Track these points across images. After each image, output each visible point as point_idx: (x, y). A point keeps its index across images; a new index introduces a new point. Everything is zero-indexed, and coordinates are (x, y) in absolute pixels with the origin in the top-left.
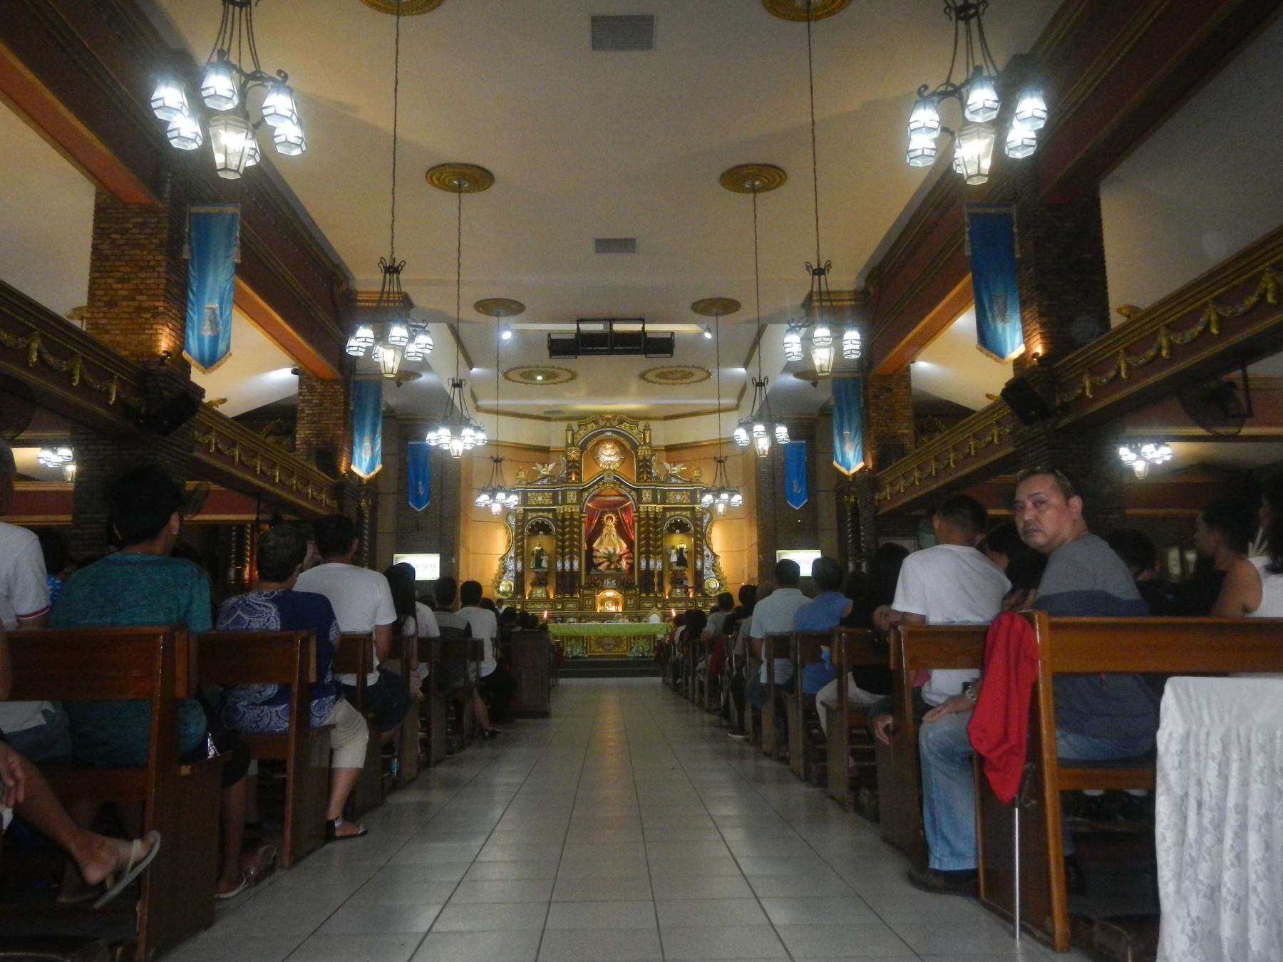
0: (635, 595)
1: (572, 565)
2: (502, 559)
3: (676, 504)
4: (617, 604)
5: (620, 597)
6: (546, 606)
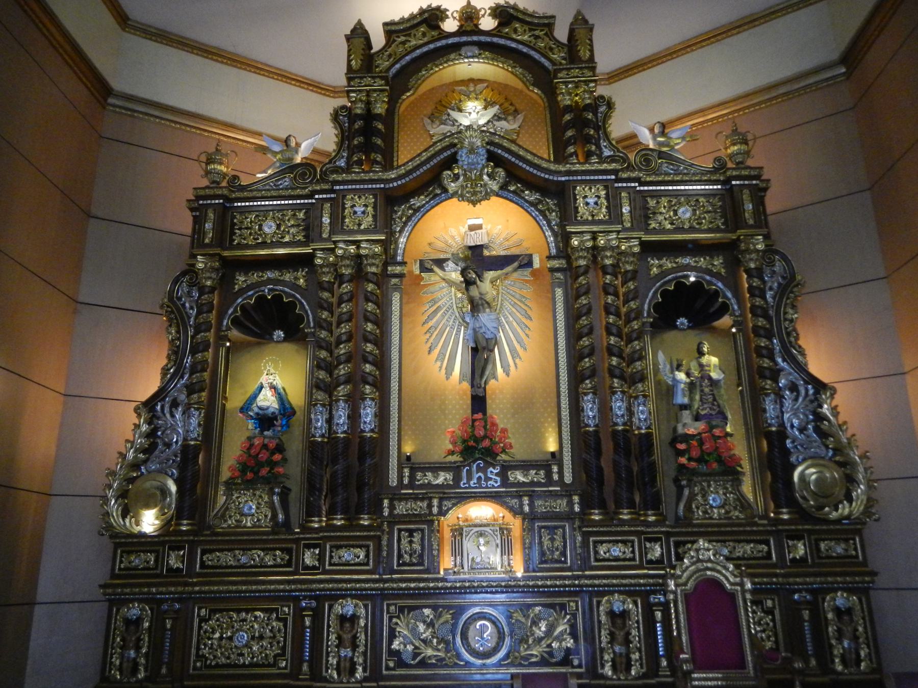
0: (569, 516)
1: (354, 417)
2: (149, 404)
3: (679, 230)
4: (506, 549)
5: (516, 525)
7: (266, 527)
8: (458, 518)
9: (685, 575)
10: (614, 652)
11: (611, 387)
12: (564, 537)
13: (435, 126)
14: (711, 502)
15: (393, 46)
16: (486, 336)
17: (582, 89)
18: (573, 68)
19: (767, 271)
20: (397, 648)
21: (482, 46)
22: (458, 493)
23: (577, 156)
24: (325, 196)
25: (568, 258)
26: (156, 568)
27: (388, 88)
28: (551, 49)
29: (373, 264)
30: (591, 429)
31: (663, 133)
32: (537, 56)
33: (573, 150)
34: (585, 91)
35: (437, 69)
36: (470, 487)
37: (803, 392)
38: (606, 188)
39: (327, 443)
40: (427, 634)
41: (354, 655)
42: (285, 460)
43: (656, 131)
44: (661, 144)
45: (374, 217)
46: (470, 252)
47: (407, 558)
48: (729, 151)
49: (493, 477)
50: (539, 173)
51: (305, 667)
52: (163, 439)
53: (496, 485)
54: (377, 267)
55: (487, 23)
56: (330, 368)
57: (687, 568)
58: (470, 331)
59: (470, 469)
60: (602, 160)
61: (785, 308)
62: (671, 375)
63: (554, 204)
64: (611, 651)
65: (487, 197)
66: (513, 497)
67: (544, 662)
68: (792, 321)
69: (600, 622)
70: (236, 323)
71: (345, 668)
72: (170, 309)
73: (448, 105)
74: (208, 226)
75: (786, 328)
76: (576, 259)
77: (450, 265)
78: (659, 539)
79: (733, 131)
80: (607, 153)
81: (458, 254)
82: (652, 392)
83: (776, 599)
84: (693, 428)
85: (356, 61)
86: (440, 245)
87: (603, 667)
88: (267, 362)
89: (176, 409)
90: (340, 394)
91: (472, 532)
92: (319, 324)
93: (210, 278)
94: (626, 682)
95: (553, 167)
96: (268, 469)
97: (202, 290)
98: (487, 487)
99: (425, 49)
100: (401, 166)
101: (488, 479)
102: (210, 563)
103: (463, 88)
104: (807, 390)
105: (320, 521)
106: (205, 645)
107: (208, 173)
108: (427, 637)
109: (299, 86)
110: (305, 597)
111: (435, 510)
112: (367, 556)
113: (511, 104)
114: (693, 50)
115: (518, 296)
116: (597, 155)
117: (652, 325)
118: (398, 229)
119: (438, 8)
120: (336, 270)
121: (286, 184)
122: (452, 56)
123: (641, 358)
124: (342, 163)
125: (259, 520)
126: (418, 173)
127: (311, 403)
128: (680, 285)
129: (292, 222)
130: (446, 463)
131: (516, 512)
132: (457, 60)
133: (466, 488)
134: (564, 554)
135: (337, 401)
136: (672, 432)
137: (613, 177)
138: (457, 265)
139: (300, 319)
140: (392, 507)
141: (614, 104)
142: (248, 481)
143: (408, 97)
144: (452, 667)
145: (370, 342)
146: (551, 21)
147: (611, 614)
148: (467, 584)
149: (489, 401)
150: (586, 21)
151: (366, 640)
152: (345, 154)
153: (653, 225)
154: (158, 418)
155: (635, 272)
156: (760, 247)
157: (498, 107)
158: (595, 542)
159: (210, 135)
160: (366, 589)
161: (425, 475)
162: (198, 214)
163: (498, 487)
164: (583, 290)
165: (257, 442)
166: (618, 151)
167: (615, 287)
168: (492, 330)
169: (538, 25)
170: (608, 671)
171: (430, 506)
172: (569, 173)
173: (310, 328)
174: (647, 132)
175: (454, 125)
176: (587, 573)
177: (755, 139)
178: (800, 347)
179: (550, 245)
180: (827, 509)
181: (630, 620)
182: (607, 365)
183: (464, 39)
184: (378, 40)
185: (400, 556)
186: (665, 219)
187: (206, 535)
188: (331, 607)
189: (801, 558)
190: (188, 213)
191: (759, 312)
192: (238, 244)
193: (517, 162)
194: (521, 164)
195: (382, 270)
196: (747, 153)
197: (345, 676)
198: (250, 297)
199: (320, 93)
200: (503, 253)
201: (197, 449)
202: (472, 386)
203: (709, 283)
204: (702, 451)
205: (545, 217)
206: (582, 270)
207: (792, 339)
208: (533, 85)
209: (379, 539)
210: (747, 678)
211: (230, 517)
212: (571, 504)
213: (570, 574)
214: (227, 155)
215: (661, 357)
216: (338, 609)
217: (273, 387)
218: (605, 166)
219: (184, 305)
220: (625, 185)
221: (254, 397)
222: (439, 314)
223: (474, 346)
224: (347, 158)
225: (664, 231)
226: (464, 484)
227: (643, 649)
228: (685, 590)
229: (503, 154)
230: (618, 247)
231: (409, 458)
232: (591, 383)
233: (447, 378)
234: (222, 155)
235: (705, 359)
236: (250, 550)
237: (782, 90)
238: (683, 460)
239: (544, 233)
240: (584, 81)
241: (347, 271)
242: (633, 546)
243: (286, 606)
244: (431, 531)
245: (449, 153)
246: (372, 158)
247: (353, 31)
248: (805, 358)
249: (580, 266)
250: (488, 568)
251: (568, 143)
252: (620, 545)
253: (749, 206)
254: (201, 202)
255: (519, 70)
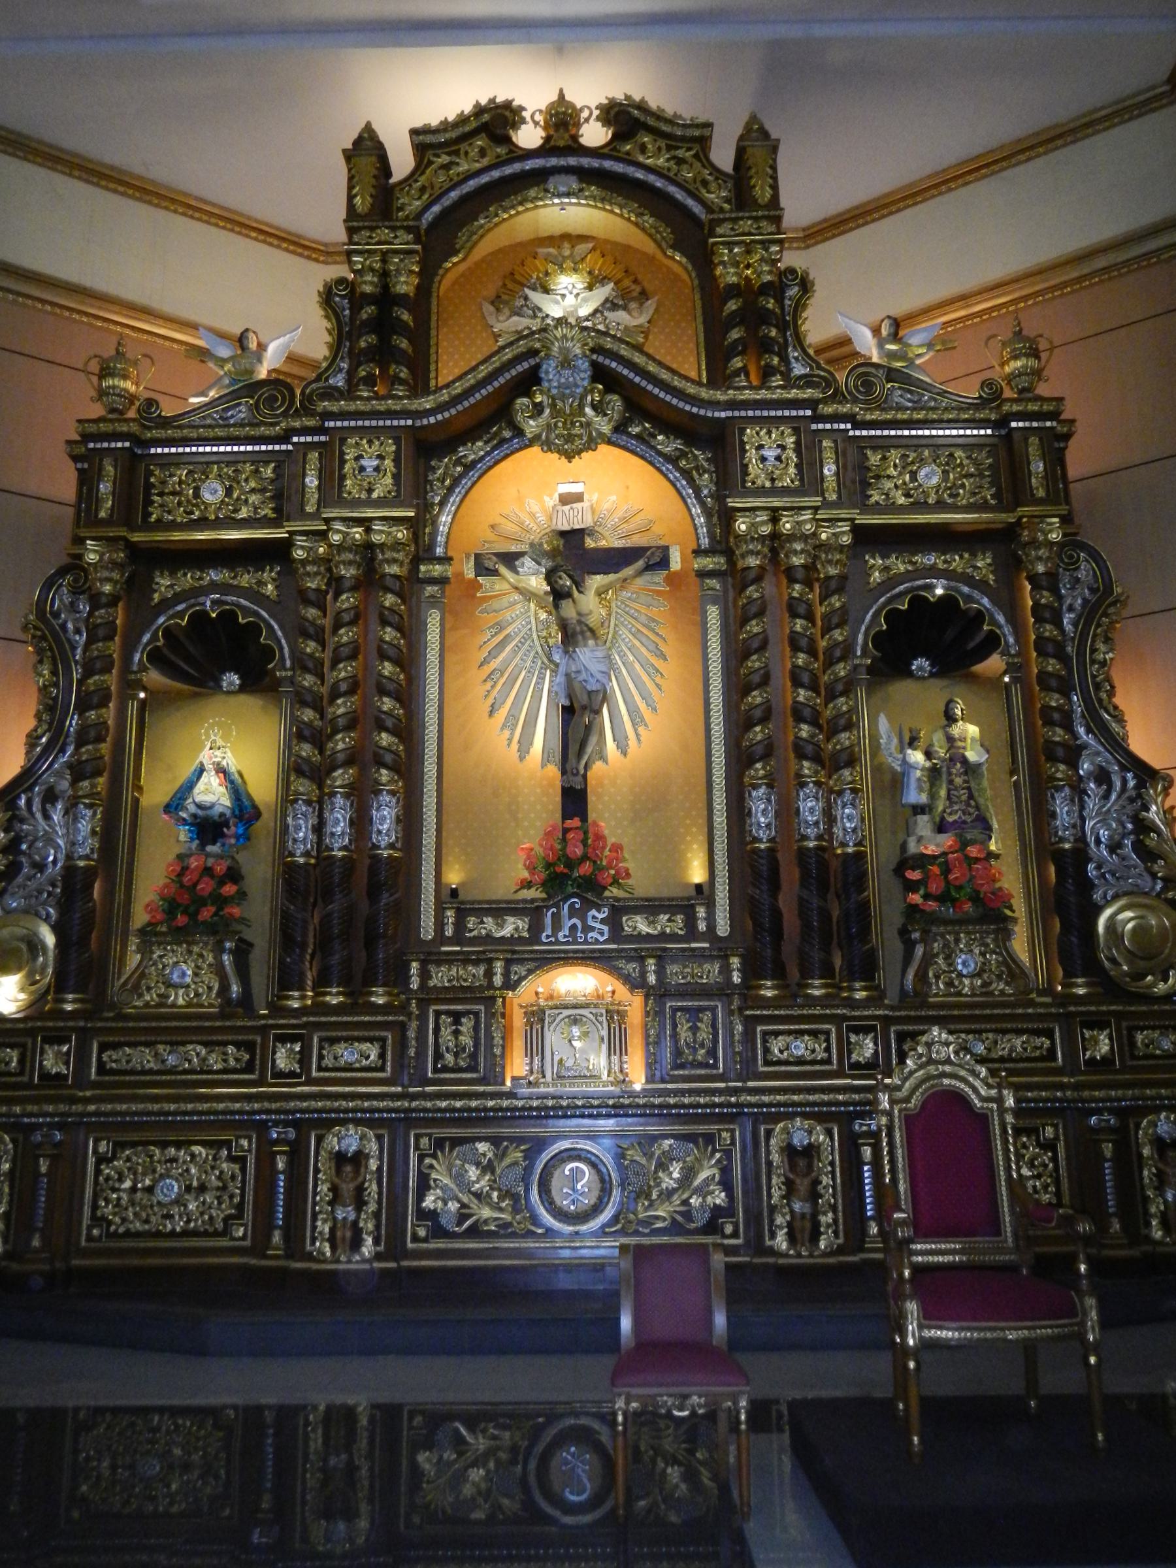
0: (723, 991)
1: (361, 822)
3: (920, 506)
4: (617, 1044)
6: (215, 1061)
7: (211, 1005)
8: (537, 993)
9: (907, 1085)
10: (792, 1212)
11: (799, 775)
12: (714, 1026)
13: (501, 318)
14: (960, 967)
15: (428, 171)
16: (589, 688)
17: (758, 257)
18: (742, 218)
19: (1065, 579)
20: (432, 1207)
21: (586, 176)
22: (536, 951)
23: (747, 375)
24: (309, 439)
25: (729, 554)
26: (21, 1073)
27: (418, 247)
28: (705, 183)
29: (395, 561)
30: (762, 846)
31: (895, 337)
32: (679, 195)
33: (740, 365)
34: (762, 259)
35: (506, 216)
36: (557, 942)
37: (1118, 784)
38: (796, 431)
39: (315, 866)
40: (482, 1185)
41: (358, 1217)
42: (242, 895)
43: (884, 332)
44: (892, 355)
45: (396, 477)
46: (562, 542)
47: (449, 1058)
48: (1007, 369)
49: (598, 925)
50: (681, 405)
51: (277, 1237)
52: (30, 856)
53: (601, 939)
54: (401, 564)
55: (594, 134)
56: (319, 739)
57: (911, 1073)
58: (560, 679)
59: (559, 912)
60: (790, 382)
61: (1093, 641)
62: (901, 756)
63: (707, 460)
64: (786, 1210)
65: (591, 445)
66: (630, 959)
67: (675, 1227)
68: (1103, 664)
69: (769, 1164)
70: (156, 658)
71: (344, 1238)
72: (39, 633)
73: (525, 282)
74: (105, 488)
75: (1094, 677)
76: (743, 556)
77: (528, 563)
78: (873, 1029)
79: (1015, 333)
80: (799, 370)
81: (541, 545)
82: (867, 784)
83: (1061, 1126)
84: (933, 844)
85: (363, 198)
86: (509, 528)
87: (773, 1236)
88: (211, 727)
89: (53, 804)
90: (337, 783)
91: (561, 1016)
92: (302, 663)
93: (109, 580)
94: (812, 1261)
95: (705, 394)
96: (213, 909)
97: (95, 601)
98: (586, 942)
99: (484, 179)
100: (442, 388)
101: (587, 929)
102: (114, 1065)
103: (551, 250)
104: (1124, 782)
105: (303, 997)
106: (107, 1201)
107: (102, 393)
108: (481, 1189)
109: (264, 242)
110: (276, 1123)
111: (498, 980)
112: (382, 1056)
113: (635, 281)
114: (950, 190)
115: (643, 619)
116: (781, 373)
117: (870, 670)
118: (437, 499)
119: (507, 105)
120: (329, 570)
121: (242, 415)
122: (532, 193)
123: (849, 726)
124: (339, 381)
125: (197, 995)
126: (472, 400)
127: (287, 799)
128: (918, 602)
129: (253, 484)
130: (518, 902)
131: (635, 983)
132: (541, 199)
133: (550, 943)
134: (713, 1053)
135: (333, 794)
136: (898, 851)
137: (809, 413)
138: (539, 564)
139: (268, 653)
140: (425, 975)
141: (813, 284)
142: (179, 929)
143: (454, 264)
144: (523, 1236)
145: (388, 694)
146: (706, 132)
147: (790, 1151)
148: (550, 1103)
149: (591, 798)
150: (765, 135)
151: (380, 1193)
152: (345, 365)
153: (876, 497)
154: (22, 821)
155: (843, 578)
156: (1054, 536)
157: (612, 285)
158: (765, 1034)
159: (105, 325)
160: (380, 1111)
161: (482, 922)
162: (86, 466)
163: (605, 942)
164: (754, 609)
165: (194, 863)
166: (819, 367)
167: (809, 605)
168: (599, 676)
169: (683, 139)
170: (781, 1242)
171: (489, 974)
172: (732, 405)
173: (286, 670)
174: (868, 334)
175: (535, 317)
176: (750, 1084)
177: (1051, 349)
178: (1116, 708)
179: (699, 531)
180: (1149, 978)
181: (819, 1160)
182: (792, 738)
183: (553, 161)
184: (402, 161)
185: (438, 1056)
186: (896, 487)
187: (107, 1019)
188: (320, 1139)
189: (1103, 1058)
190: (72, 464)
191: (1050, 648)
192: (159, 521)
193: (644, 383)
194: (650, 387)
195: (410, 571)
196: (1037, 373)
197: (345, 1252)
198: (180, 615)
199: (301, 255)
200: (618, 544)
201: (90, 874)
202: (564, 772)
203: (969, 599)
204: (948, 882)
205: (691, 482)
206: (752, 575)
207: (1104, 696)
208: (674, 247)
209: (403, 1027)
210: (1001, 1251)
211: (149, 989)
212: (726, 970)
213: (722, 1085)
214: (135, 363)
215: (883, 724)
216: (332, 1142)
217: (221, 771)
218: (794, 393)
219: (63, 627)
220: (828, 426)
221: (190, 786)
222: (508, 649)
223: (567, 703)
224: (348, 372)
225: (891, 508)
226: (548, 937)
227: (840, 1208)
228: (905, 1109)
229: (620, 369)
230: (815, 535)
231: (454, 893)
232: (764, 768)
233: (522, 758)
234: (127, 361)
235: (956, 730)
236: (184, 1044)
237: (1101, 262)
238: (916, 898)
239: (689, 510)
240: (762, 242)
241: (348, 572)
242: (828, 1040)
243: (245, 1137)
244: (491, 1015)
245: (526, 365)
246: (391, 372)
247: (358, 142)
248: (1124, 727)
249: (749, 568)
250: (585, 1076)
251: (732, 351)
252: (806, 1038)
253: (1038, 467)
254: (91, 445)
255: (649, 221)
